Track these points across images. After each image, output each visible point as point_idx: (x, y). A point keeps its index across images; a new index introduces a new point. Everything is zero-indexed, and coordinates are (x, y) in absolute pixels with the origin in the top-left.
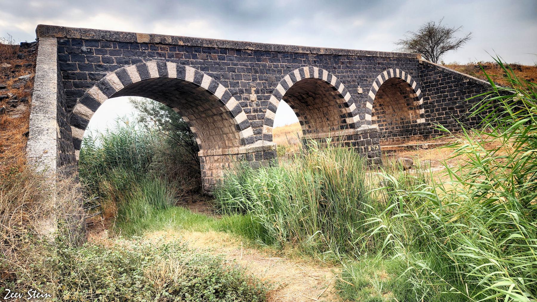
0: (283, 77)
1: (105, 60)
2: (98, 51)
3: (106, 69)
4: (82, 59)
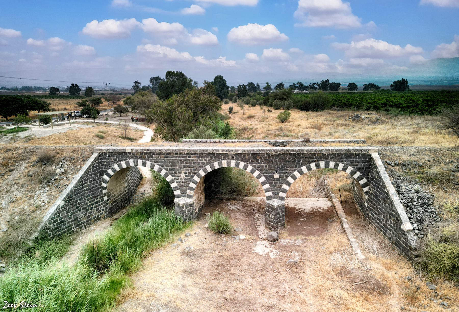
0: (205, 166)
1: (114, 160)
2: (112, 156)
3: (114, 163)
4: (107, 159)
